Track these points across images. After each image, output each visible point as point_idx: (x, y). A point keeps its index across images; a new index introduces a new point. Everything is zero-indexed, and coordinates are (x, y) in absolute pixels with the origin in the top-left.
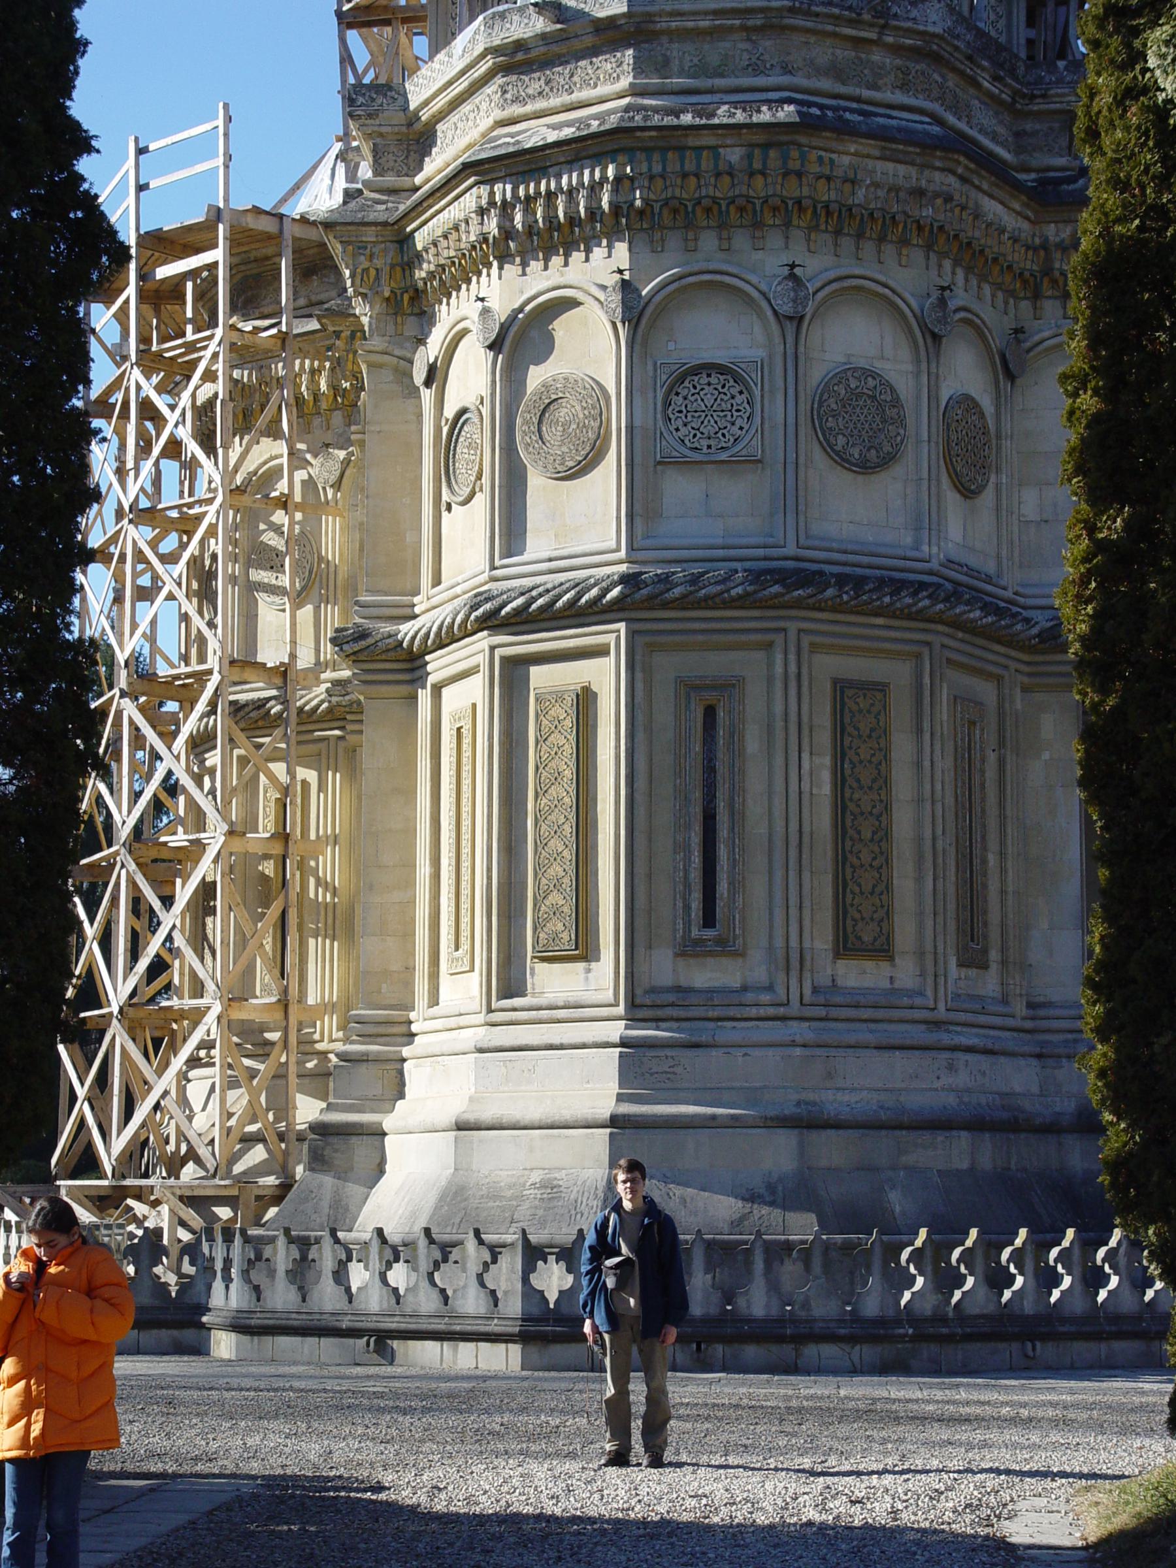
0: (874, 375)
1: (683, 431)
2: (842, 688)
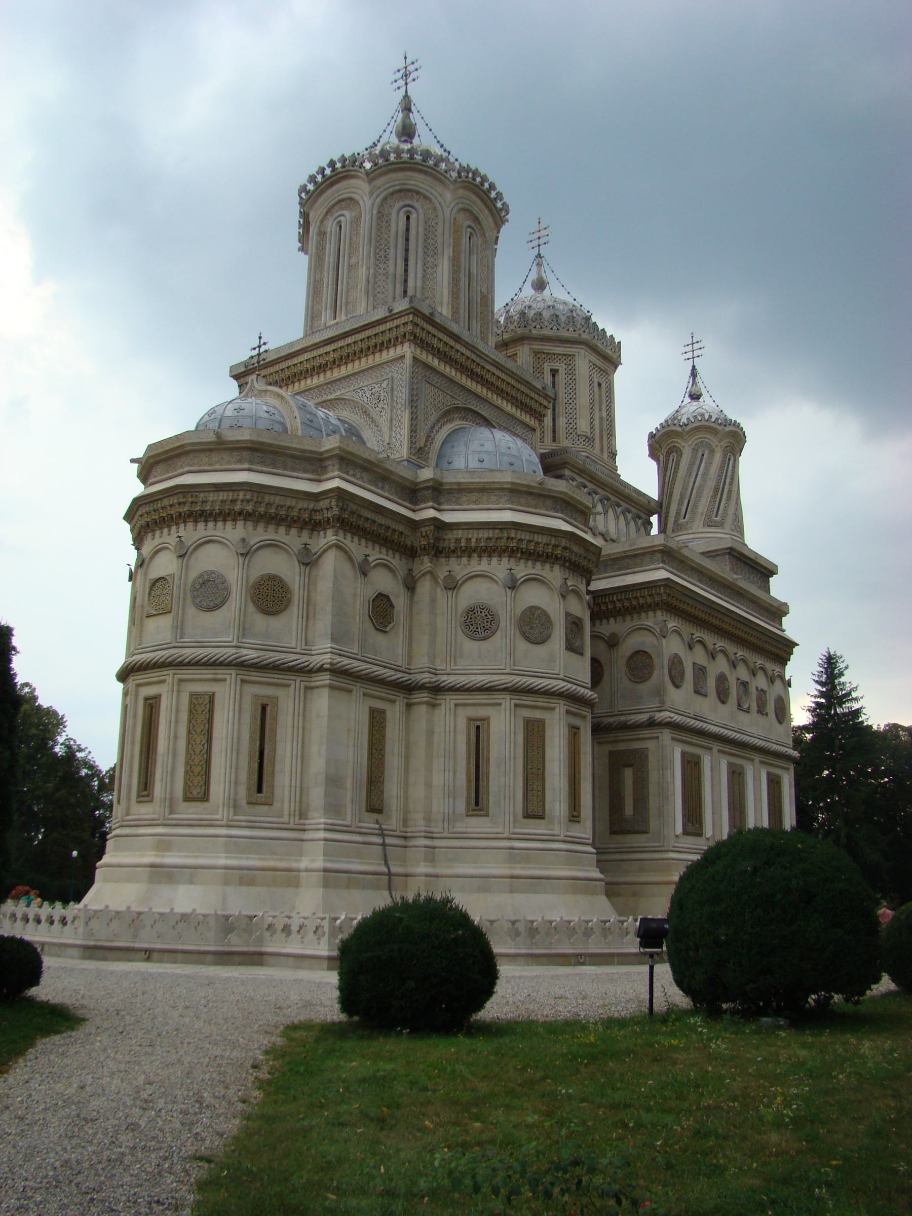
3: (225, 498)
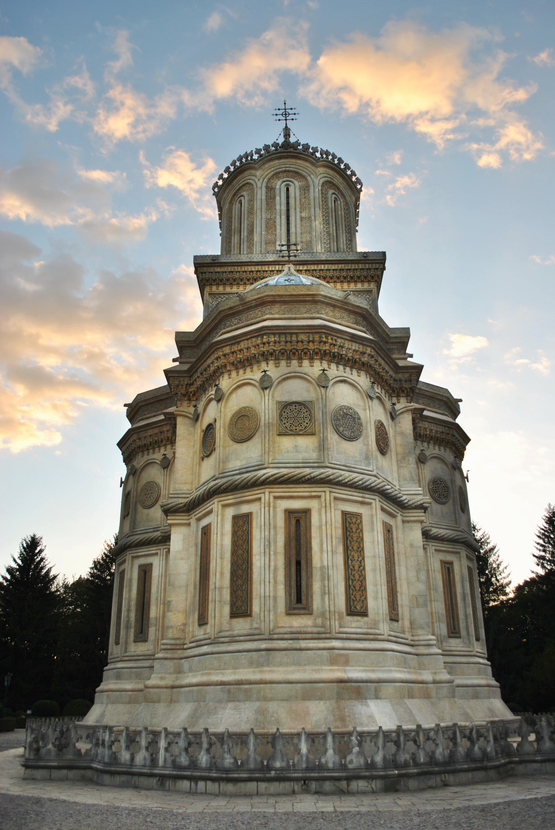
0: (351, 409)
2: (345, 514)
3: (357, 349)
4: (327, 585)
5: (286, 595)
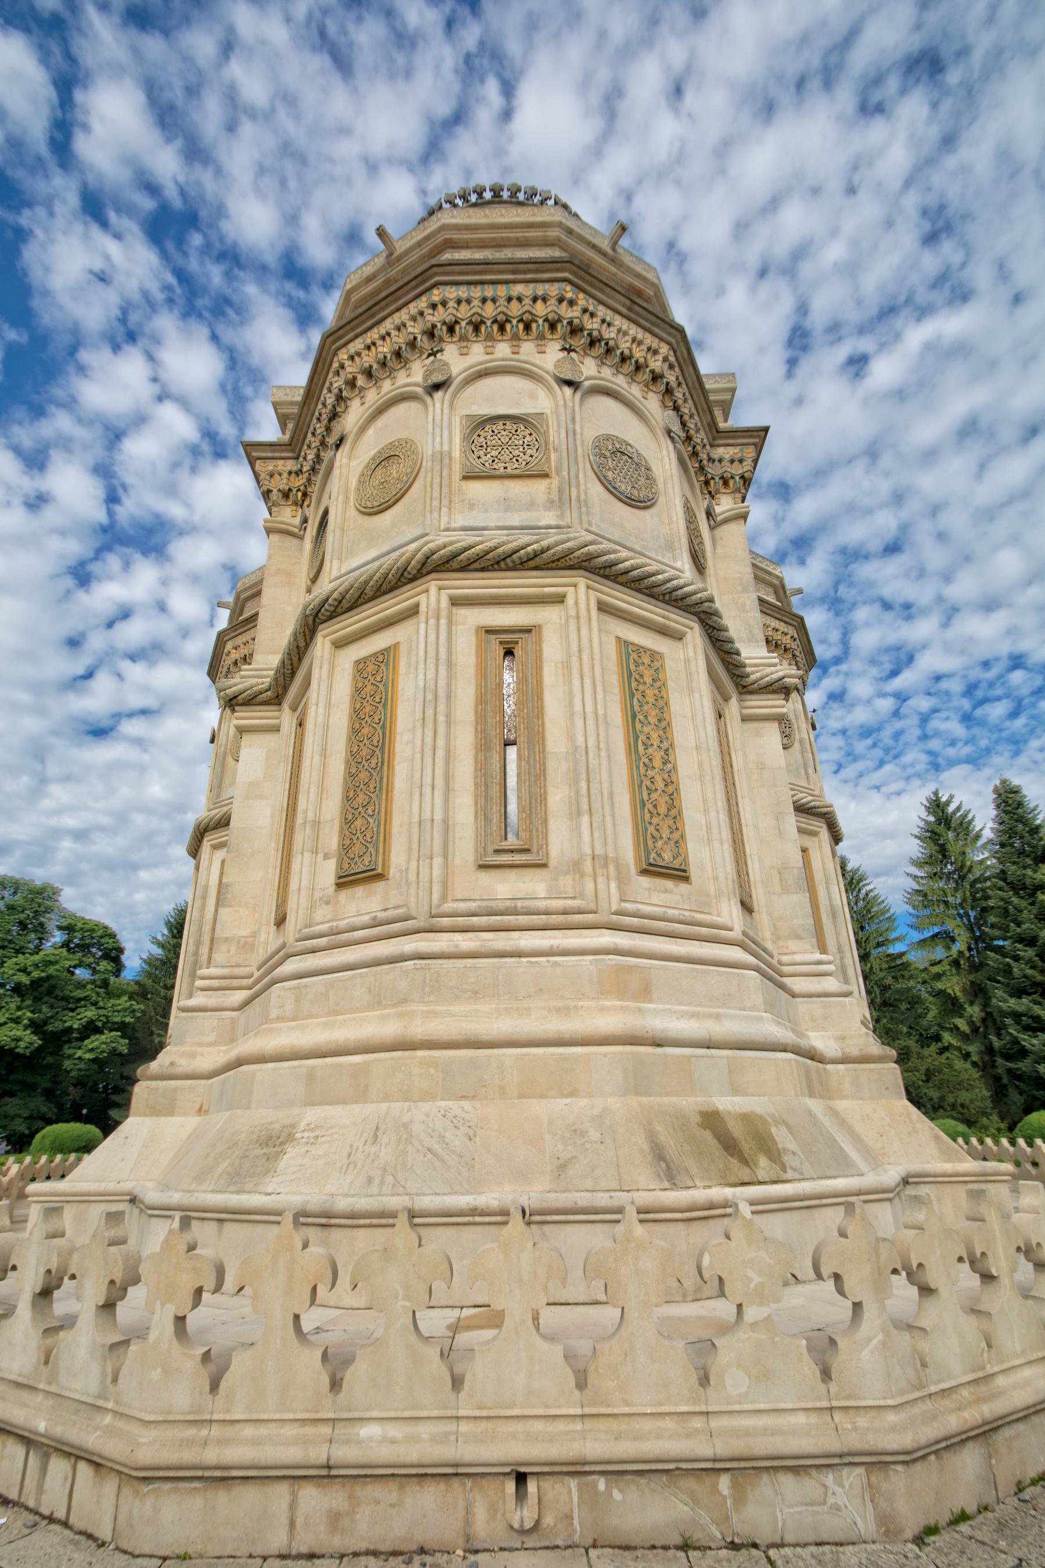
1: (484, 458)
4: (584, 791)
5: (476, 818)
